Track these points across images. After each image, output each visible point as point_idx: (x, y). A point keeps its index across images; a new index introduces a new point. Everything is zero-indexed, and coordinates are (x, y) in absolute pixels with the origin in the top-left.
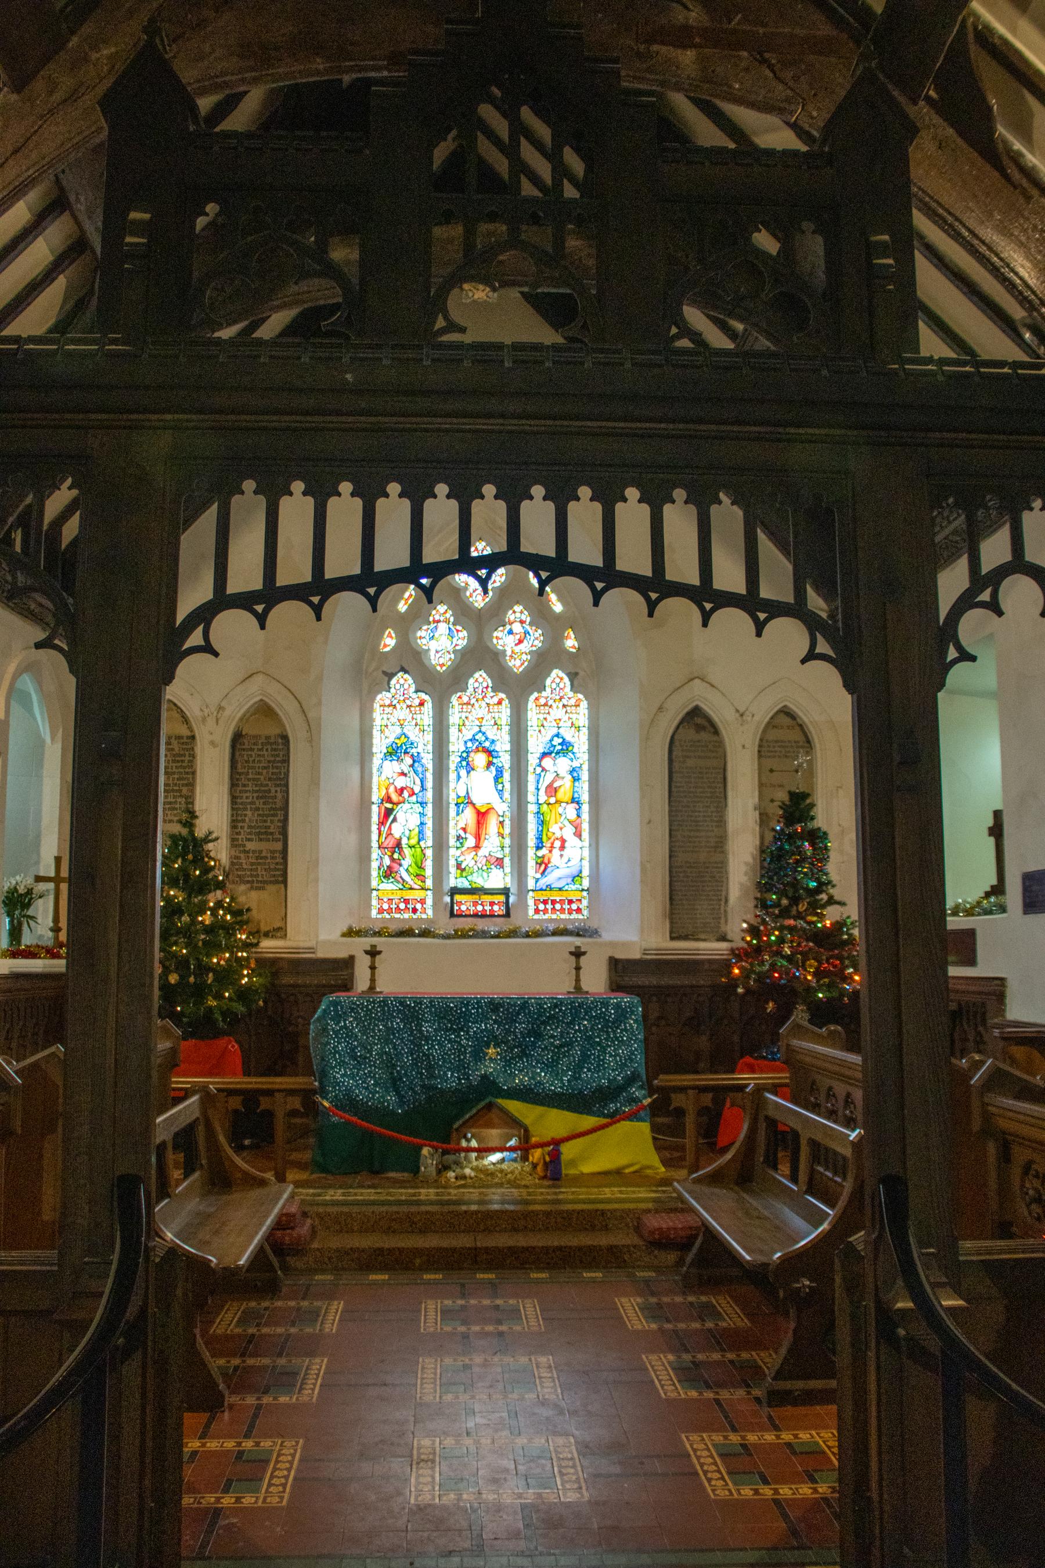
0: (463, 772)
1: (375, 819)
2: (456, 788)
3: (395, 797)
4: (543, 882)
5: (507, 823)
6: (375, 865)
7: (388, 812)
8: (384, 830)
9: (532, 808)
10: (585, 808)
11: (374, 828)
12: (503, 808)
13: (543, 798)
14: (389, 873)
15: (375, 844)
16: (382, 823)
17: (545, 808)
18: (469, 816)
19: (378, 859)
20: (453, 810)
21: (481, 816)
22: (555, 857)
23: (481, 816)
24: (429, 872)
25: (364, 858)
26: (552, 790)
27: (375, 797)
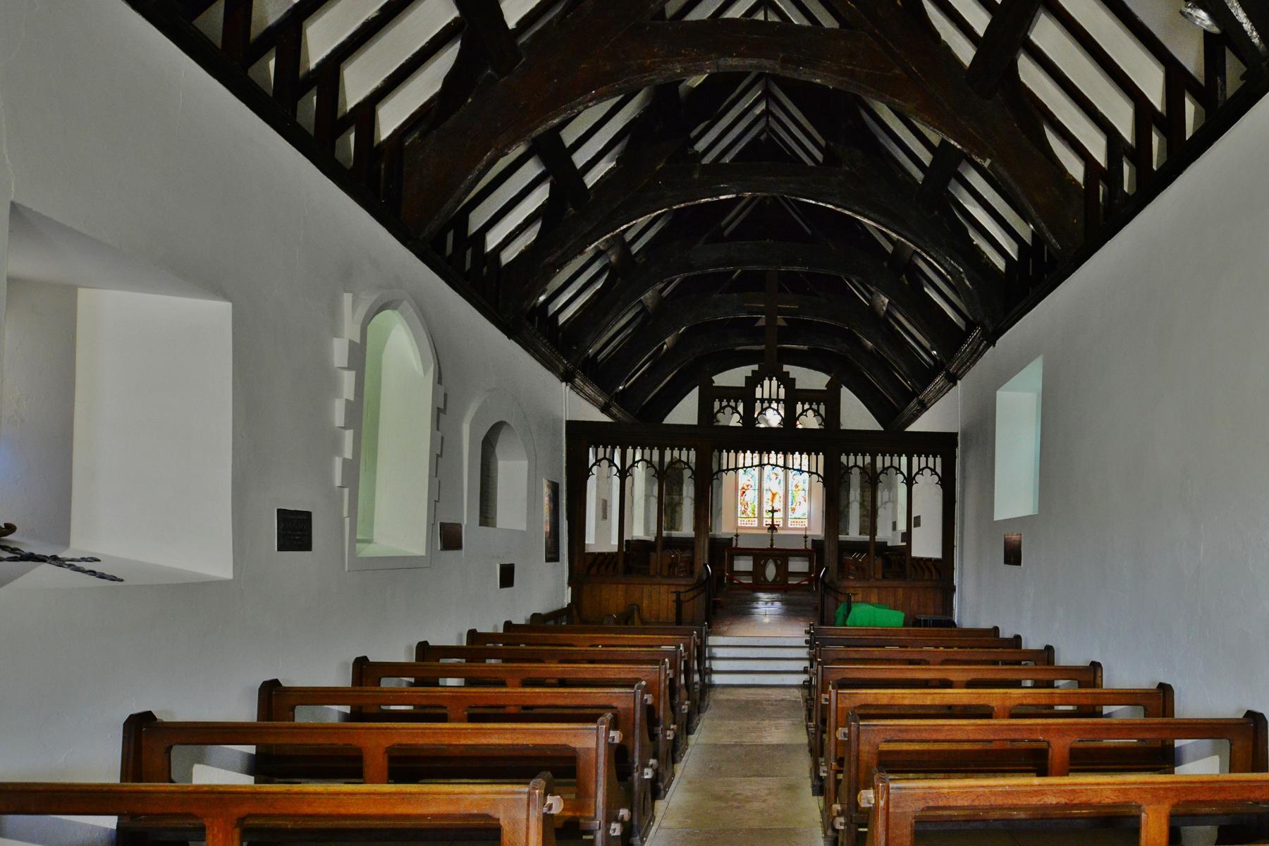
0: (768, 481)
1: (740, 493)
2: (766, 485)
3: (746, 488)
4: (793, 516)
5: (782, 498)
6: (739, 510)
7: (744, 492)
8: (742, 498)
9: (790, 492)
10: (807, 492)
11: (739, 497)
12: (781, 493)
13: (794, 489)
14: (744, 512)
15: (739, 503)
16: (742, 496)
17: (794, 492)
18: (770, 496)
19: (740, 508)
20: (765, 491)
21: (774, 495)
22: (797, 508)
23: (774, 495)
24: (756, 512)
25: (736, 507)
26: (797, 486)
27: (740, 488)
